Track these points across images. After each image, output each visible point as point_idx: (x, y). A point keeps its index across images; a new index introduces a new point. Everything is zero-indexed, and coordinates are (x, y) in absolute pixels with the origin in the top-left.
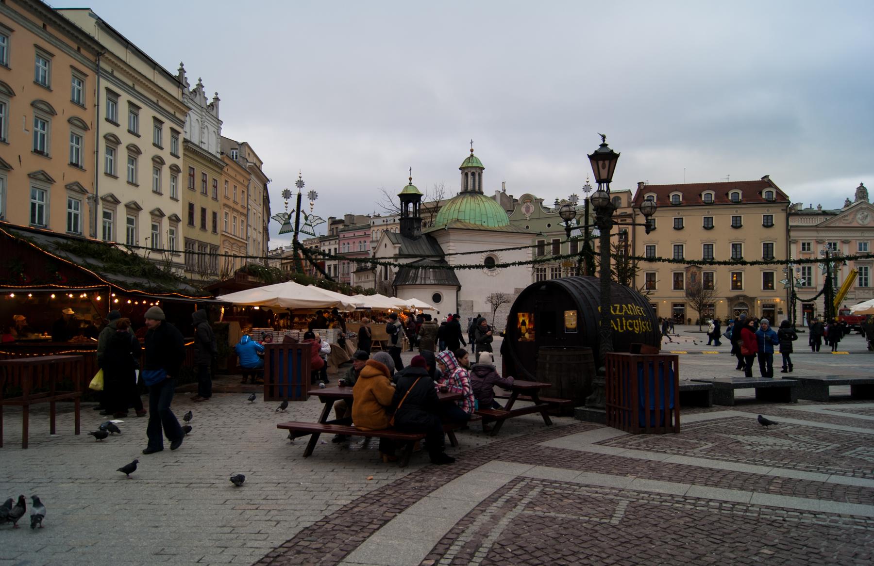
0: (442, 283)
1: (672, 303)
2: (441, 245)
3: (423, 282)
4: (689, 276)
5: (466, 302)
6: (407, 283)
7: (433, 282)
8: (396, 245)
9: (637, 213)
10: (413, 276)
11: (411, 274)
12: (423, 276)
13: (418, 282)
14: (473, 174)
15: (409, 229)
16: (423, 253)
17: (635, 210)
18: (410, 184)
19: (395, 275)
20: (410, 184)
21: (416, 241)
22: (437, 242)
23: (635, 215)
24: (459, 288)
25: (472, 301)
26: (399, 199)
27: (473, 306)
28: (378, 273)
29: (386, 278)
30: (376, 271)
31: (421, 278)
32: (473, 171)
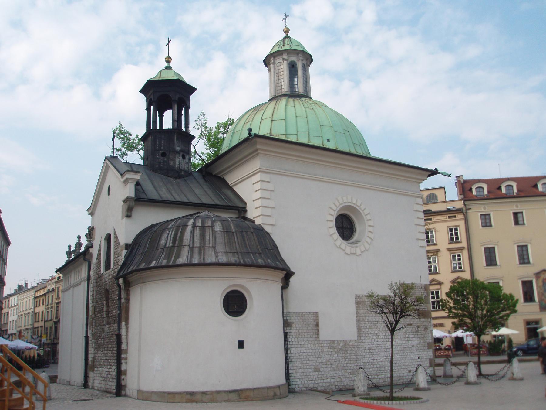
0: (248, 260)
1: (524, 320)
2: (236, 188)
3: (196, 260)
4: (541, 284)
5: (301, 315)
6: (153, 264)
7: (223, 259)
8: (127, 176)
9: (468, 207)
10: (170, 244)
11: (163, 241)
12: (197, 244)
13: (182, 260)
14: (293, 67)
15: (164, 155)
16: (193, 200)
17: (466, 203)
18: (168, 68)
19: (124, 252)
20: (168, 68)
21: (179, 180)
22: (226, 184)
23: (467, 209)
24: (288, 275)
25: (316, 314)
26: (142, 98)
27: (317, 325)
28: (94, 260)
29: (108, 267)
30: (91, 255)
31: (191, 249)
32: (293, 58)
